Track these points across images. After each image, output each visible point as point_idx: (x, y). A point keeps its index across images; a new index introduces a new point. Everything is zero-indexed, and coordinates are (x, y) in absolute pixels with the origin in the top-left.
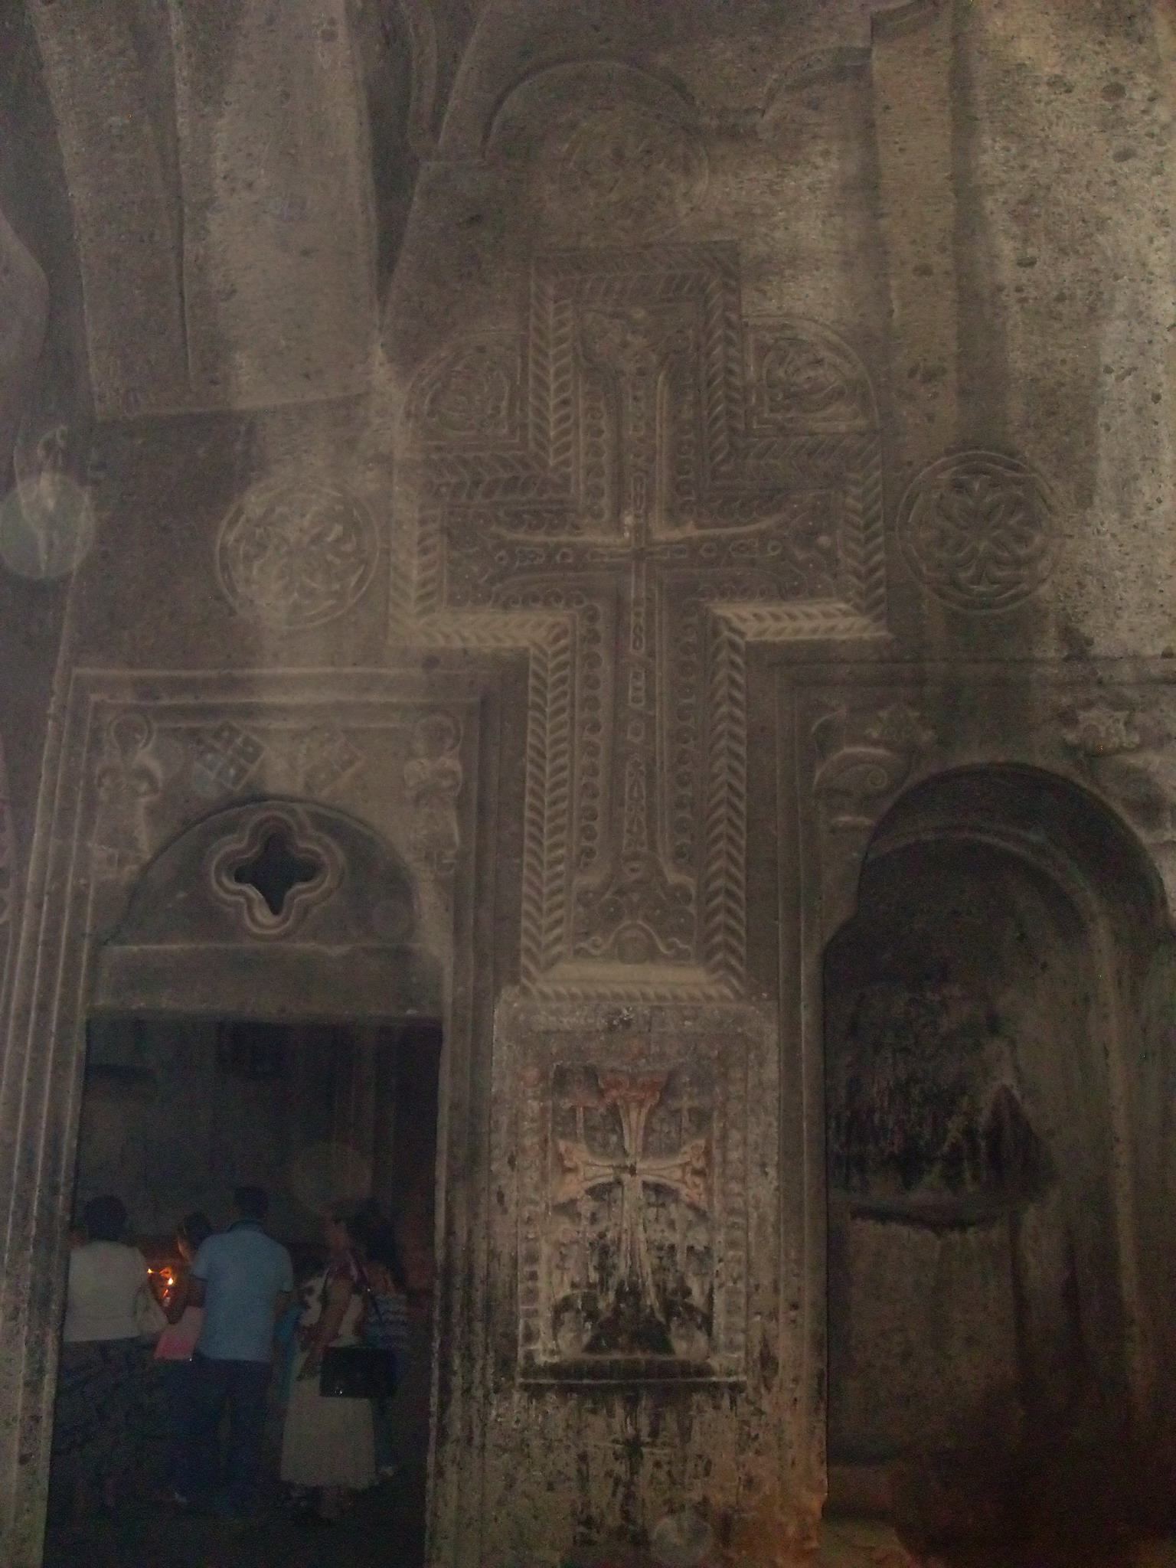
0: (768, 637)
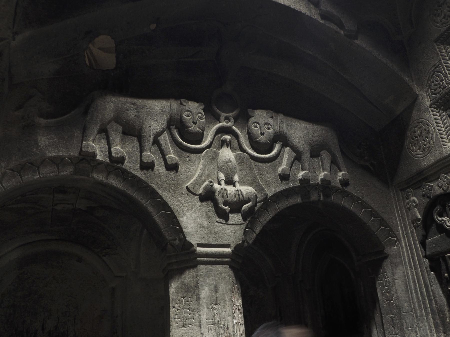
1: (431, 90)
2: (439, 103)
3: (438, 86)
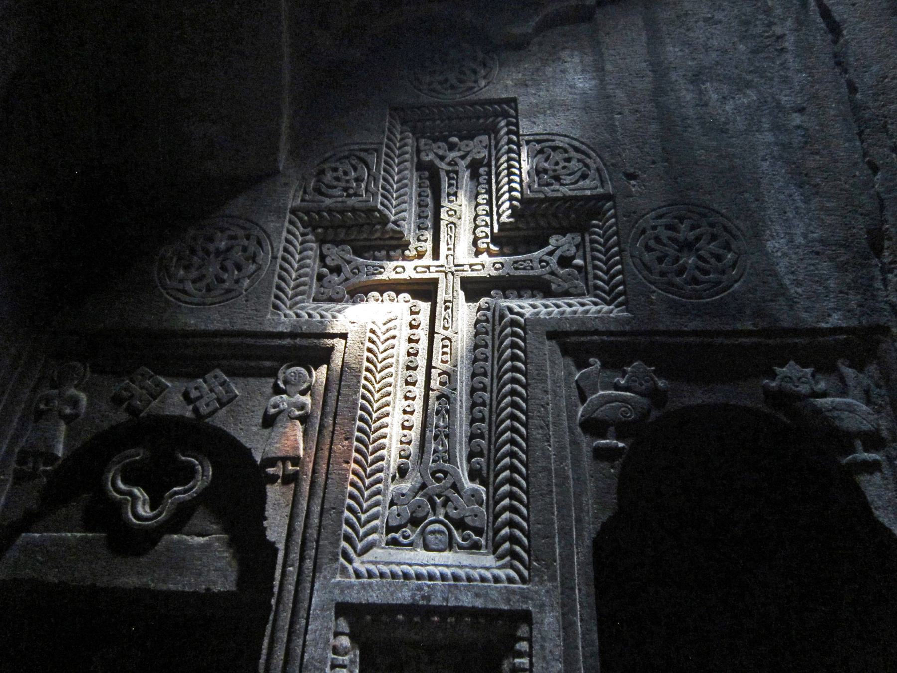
0: (542, 316)
1: (319, 181)
2: (321, 217)
3: (344, 184)
